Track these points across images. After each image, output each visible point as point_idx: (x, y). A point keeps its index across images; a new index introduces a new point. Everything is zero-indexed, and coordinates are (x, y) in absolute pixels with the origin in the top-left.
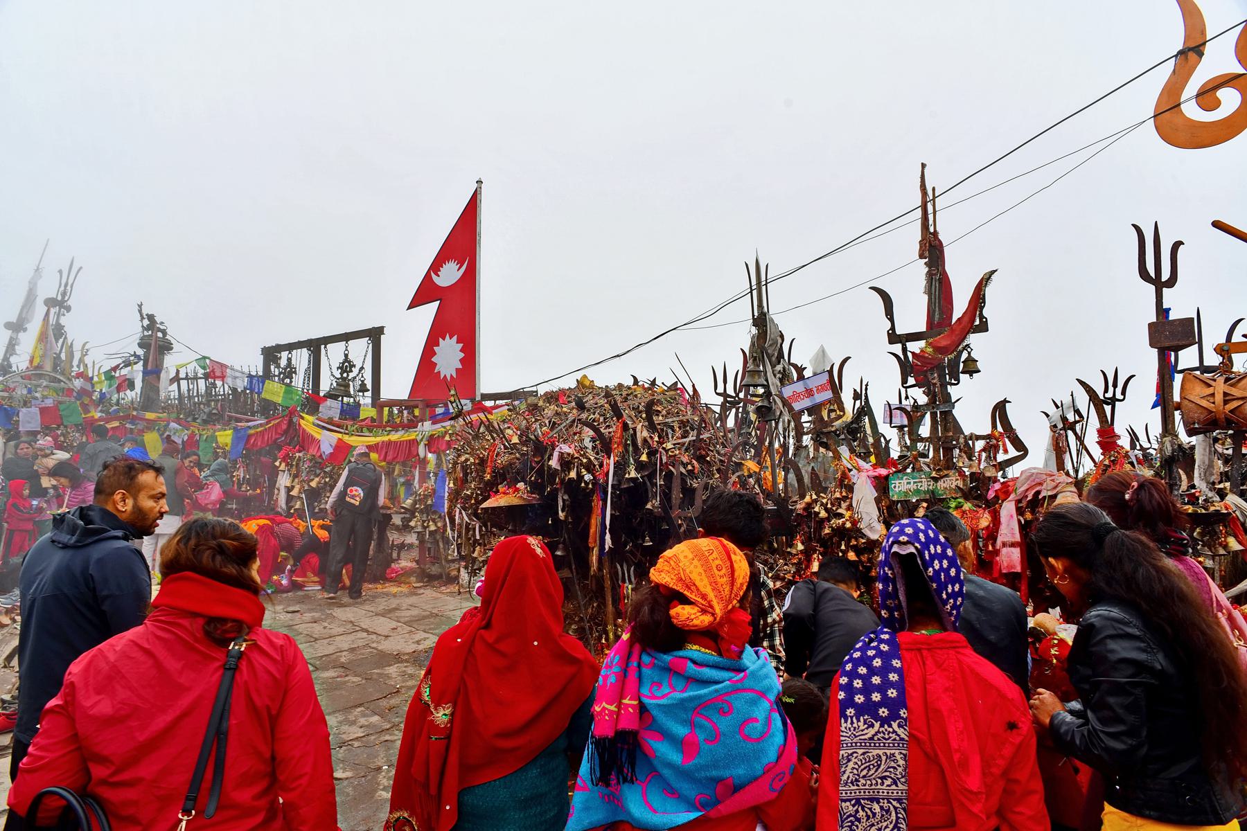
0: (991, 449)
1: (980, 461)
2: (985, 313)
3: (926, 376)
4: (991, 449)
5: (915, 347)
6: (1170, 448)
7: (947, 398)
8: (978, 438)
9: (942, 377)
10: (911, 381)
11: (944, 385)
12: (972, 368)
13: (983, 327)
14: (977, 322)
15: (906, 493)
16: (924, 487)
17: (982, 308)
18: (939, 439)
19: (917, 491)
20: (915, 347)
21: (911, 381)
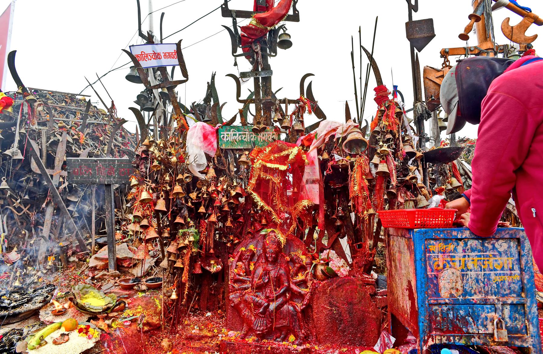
0: (299, 112)
1: (291, 121)
2: (298, 6)
3: (251, 47)
4: (299, 112)
5: (243, 22)
6: (420, 109)
7: (267, 68)
8: (290, 102)
9: (263, 50)
10: (240, 51)
11: (265, 58)
12: (286, 44)
13: (295, 18)
14: (291, 12)
15: (232, 143)
16: (247, 138)
17: (295, 3)
18: (261, 101)
19: (242, 142)
20: (243, 22)
21: (240, 51)
